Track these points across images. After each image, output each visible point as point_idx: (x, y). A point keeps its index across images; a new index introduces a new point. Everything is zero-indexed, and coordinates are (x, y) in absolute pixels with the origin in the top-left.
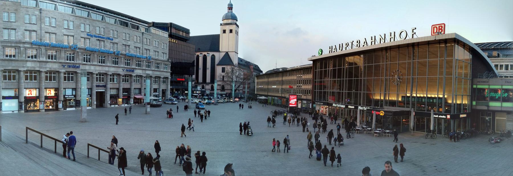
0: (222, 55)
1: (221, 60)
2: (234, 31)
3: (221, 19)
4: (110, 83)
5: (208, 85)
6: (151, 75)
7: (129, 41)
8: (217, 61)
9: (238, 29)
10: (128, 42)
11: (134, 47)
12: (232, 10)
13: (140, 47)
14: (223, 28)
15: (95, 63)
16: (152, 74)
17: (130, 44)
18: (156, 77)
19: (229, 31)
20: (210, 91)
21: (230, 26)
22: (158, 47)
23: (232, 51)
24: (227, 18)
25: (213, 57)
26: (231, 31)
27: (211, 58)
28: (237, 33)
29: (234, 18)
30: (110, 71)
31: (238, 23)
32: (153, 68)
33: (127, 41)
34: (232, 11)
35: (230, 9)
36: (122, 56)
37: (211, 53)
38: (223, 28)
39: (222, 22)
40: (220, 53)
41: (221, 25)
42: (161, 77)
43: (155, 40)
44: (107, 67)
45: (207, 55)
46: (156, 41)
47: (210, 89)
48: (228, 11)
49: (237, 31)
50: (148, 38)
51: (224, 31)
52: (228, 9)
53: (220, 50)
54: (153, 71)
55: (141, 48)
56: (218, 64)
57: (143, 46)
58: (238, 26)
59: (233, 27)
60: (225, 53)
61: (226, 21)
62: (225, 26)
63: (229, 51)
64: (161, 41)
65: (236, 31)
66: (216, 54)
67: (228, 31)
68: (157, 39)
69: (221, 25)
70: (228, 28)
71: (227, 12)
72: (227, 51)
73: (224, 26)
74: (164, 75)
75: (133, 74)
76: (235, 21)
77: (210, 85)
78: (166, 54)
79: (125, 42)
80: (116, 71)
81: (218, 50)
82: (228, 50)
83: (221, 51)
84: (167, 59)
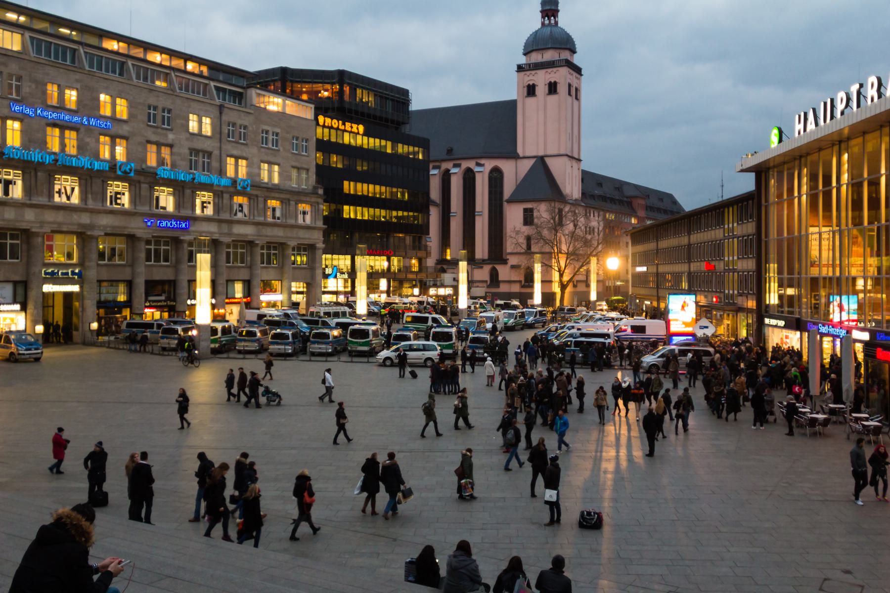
0: (525, 166)
1: (519, 184)
2: (562, 89)
3: (521, 49)
4: (98, 265)
5: (482, 267)
6: (250, 238)
7: (168, 132)
8: (509, 188)
9: (579, 79)
10: (166, 136)
11: (187, 151)
12: (555, 18)
13: (210, 149)
14: (527, 79)
15: (40, 199)
16: (254, 235)
17: (173, 140)
18: (269, 246)
19: (547, 86)
20: (488, 287)
21: (549, 70)
22: (279, 150)
23: (555, 152)
24: (540, 47)
25: (496, 177)
26: (552, 88)
27: (490, 179)
28: (575, 93)
29: (566, 44)
30: (99, 227)
31: (577, 60)
32: (259, 215)
33: (165, 132)
34: (556, 23)
35: (550, 14)
36: (142, 179)
37: (489, 164)
38: (527, 79)
39: (523, 60)
40: (520, 162)
41: (520, 68)
42: (289, 243)
43: (266, 128)
44: (88, 214)
45: (477, 169)
46: (267, 132)
47: (486, 282)
48: (543, 24)
49: (574, 85)
50: (239, 122)
51: (531, 90)
52: (543, 17)
53: (520, 151)
54: (260, 227)
55: (216, 153)
56: (512, 195)
57: (222, 146)
58: (578, 70)
59: (561, 75)
60: (532, 161)
61: (536, 57)
62: (533, 72)
63: (549, 153)
64: (288, 133)
65: (570, 85)
66: (507, 167)
67: (541, 90)
68: (275, 126)
69: (520, 68)
70: (541, 79)
71: (539, 26)
72: (541, 153)
73: (528, 73)
74: (299, 238)
75: (184, 235)
76: (565, 55)
77: (487, 268)
78: (308, 170)
79: (154, 133)
80: (118, 227)
81: (514, 156)
82: (545, 149)
83: (521, 155)
84: (311, 188)
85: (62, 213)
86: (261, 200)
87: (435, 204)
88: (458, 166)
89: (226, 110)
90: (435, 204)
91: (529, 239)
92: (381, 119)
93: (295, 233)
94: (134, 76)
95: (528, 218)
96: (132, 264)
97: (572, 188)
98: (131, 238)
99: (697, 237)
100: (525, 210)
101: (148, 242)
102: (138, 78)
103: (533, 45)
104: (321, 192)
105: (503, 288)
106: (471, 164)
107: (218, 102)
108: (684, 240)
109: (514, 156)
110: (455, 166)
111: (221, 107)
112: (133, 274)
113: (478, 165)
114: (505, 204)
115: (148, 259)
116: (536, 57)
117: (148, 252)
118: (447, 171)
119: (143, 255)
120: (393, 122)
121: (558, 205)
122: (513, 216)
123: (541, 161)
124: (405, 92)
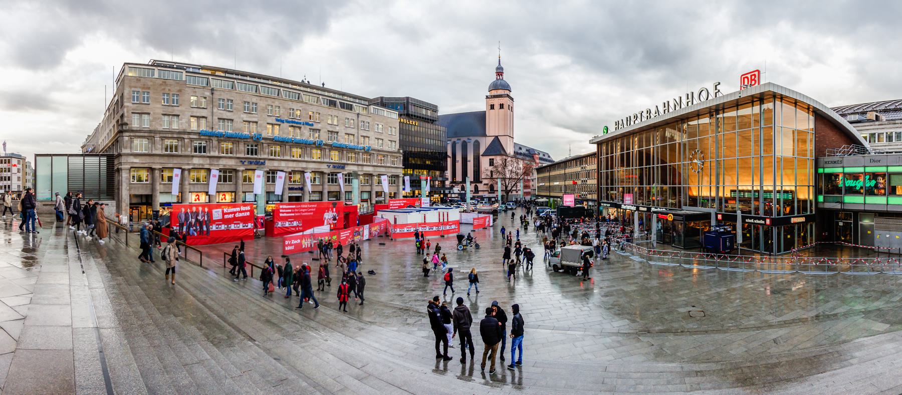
0: (489, 140)
2: (506, 106)
6: (371, 173)
8: (482, 150)
25: (477, 145)
26: (502, 106)
27: (474, 145)
28: (511, 108)
29: (507, 87)
31: (511, 95)
36: (326, 147)
37: (473, 139)
39: (488, 94)
40: (487, 138)
41: (487, 97)
48: (497, 78)
49: (511, 106)
50: (366, 121)
51: (492, 107)
53: (487, 134)
55: (356, 135)
58: (512, 99)
59: (505, 101)
60: (494, 137)
61: (494, 93)
67: (497, 107)
69: (487, 97)
70: (497, 102)
71: (495, 79)
76: (507, 92)
81: (485, 135)
85: (295, 163)
86: (375, 155)
87: (450, 157)
88: (460, 140)
89: (360, 116)
90: (450, 157)
91: (492, 172)
92: (426, 119)
93: (390, 170)
94: (322, 102)
95: (491, 163)
96: (323, 185)
97: (510, 150)
98: (322, 173)
99: (568, 171)
100: (490, 159)
101: (329, 175)
102: (324, 104)
103: (495, 86)
104: (401, 151)
105: (480, 194)
106: (465, 139)
107: (357, 112)
108: (562, 172)
109: (485, 135)
110: (458, 140)
111: (358, 114)
112: (323, 188)
113: (468, 139)
114: (481, 157)
115: (329, 182)
116: (494, 93)
117: (329, 178)
118: (454, 142)
119: (327, 180)
120: (431, 120)
121: (504, 157)
122: (485, 162)
123: (497, 137)
124: (436, 107)
